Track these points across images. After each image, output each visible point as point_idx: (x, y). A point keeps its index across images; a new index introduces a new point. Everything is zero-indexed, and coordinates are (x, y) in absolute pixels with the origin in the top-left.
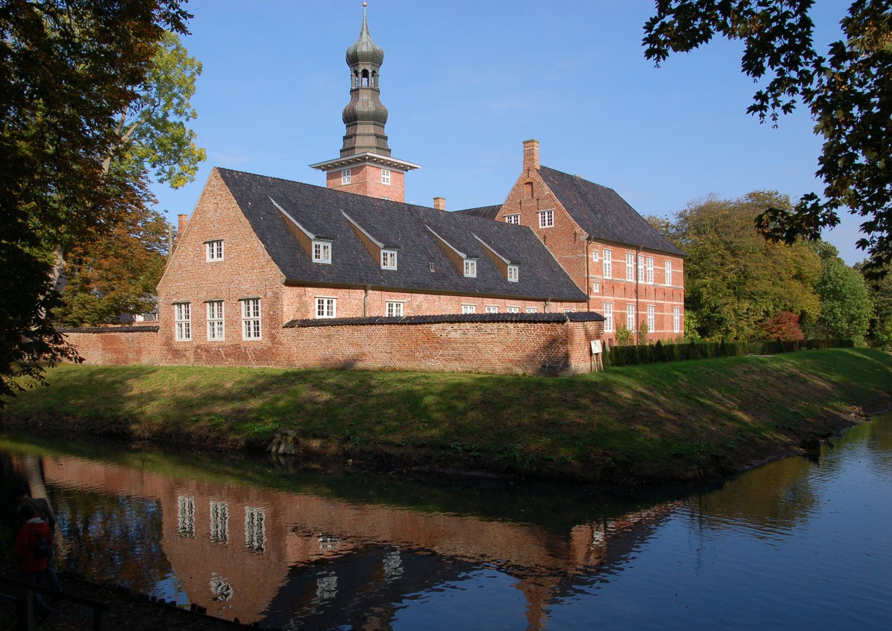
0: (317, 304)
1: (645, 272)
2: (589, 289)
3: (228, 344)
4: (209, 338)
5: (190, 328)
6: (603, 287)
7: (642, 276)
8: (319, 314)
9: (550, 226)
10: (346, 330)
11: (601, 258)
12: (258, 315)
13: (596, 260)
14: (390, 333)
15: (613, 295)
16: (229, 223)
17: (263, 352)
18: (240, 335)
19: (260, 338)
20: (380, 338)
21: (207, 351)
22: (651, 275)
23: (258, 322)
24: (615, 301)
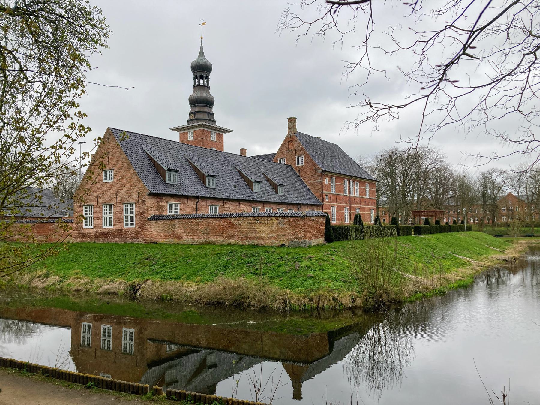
0: (168, 207)
2: (323, 200)
4: (104, 227)
5: (92, 220)
6: (331, 198)
8: (170, 212)
9: (302, 165)
10: (184, 222)
12: (133, 213)
13: (327, 184)
14: (209, 223)
15: (336, 202)
17: (136, 235)
18: (122, 224)
19: (134, 226)
21: (102, 234)
23: (133, 217)
24: (338, 205)
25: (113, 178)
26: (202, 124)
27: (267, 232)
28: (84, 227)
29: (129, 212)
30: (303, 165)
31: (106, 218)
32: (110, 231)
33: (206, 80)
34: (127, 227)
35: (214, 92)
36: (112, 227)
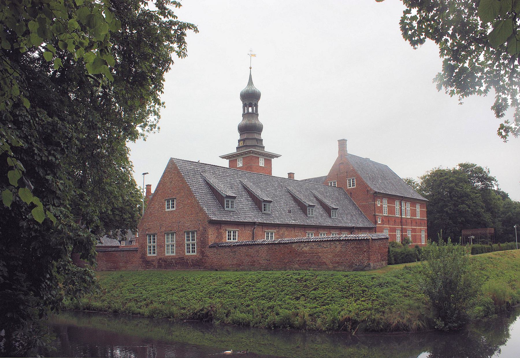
0: (227, 234)
1: (406, 211)
2: (376, 222)
3: (177, 257)
4: (166, 255)
5: (156, 248)
6: (383, 220)
7: (404, 213)
8: (228, 239)
9: (354, 187)
10: (244, 249)
11: (381, 204)
12: (194, 241)
13: (379, 205)
14: (269, 249)
16: (179, 189)
20: (264, 252)
21: (165, 261)
22: (409, 213)
23: (194, 244)
25: (175, 207)
26: (251, 150)
27: (329, 256)
28: (148, 255)
29: (191, 240)
30: (355, 187)
31: (150, 247)
32: (172, 259)
33: (255, 107)
34: (188, 254)
35: (262, 119)
36: (174, 254)
